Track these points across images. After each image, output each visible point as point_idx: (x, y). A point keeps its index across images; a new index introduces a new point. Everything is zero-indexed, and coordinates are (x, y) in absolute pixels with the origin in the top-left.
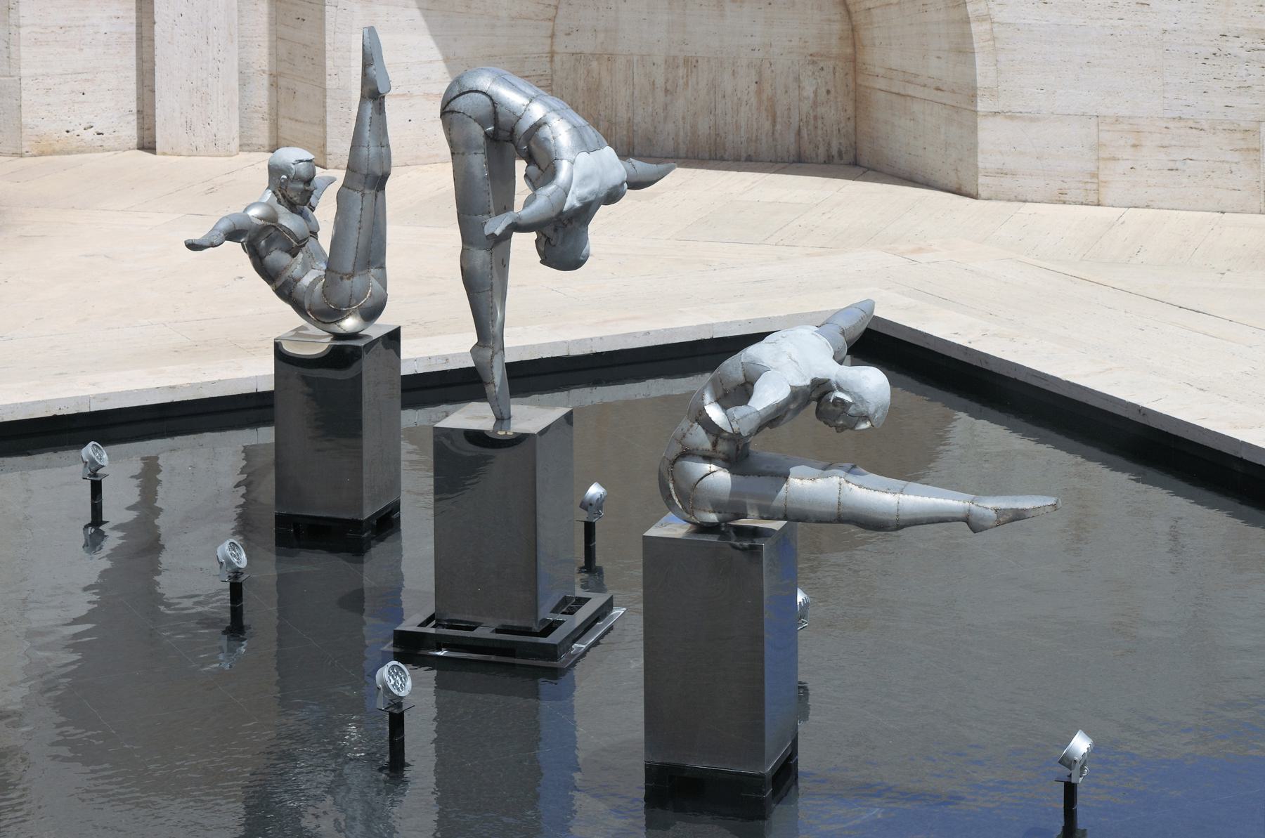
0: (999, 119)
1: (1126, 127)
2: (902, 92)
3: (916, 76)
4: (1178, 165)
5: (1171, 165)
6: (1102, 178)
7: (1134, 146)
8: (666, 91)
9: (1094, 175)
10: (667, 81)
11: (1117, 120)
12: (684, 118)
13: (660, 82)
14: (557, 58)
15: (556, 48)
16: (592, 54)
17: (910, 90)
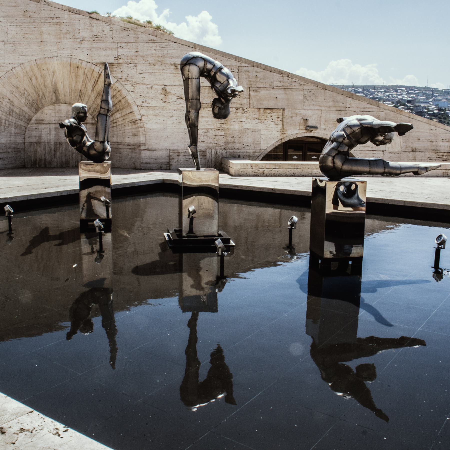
0: (146, 151)
1: (176, 151)
2: (117, 147)
3: (121, 143)
4: (188, 160)
5: (186, 160)
6: (170, 163)
7: (178, 156)
8: (54, 151)
9: (169, 163)
10: (54, 148)
11: (174, 150)
12: (59, 157)
13: (53, 148)
14: (26, 144)
15: (26, 142)
16: (35, 143)
17: (120, 147)
